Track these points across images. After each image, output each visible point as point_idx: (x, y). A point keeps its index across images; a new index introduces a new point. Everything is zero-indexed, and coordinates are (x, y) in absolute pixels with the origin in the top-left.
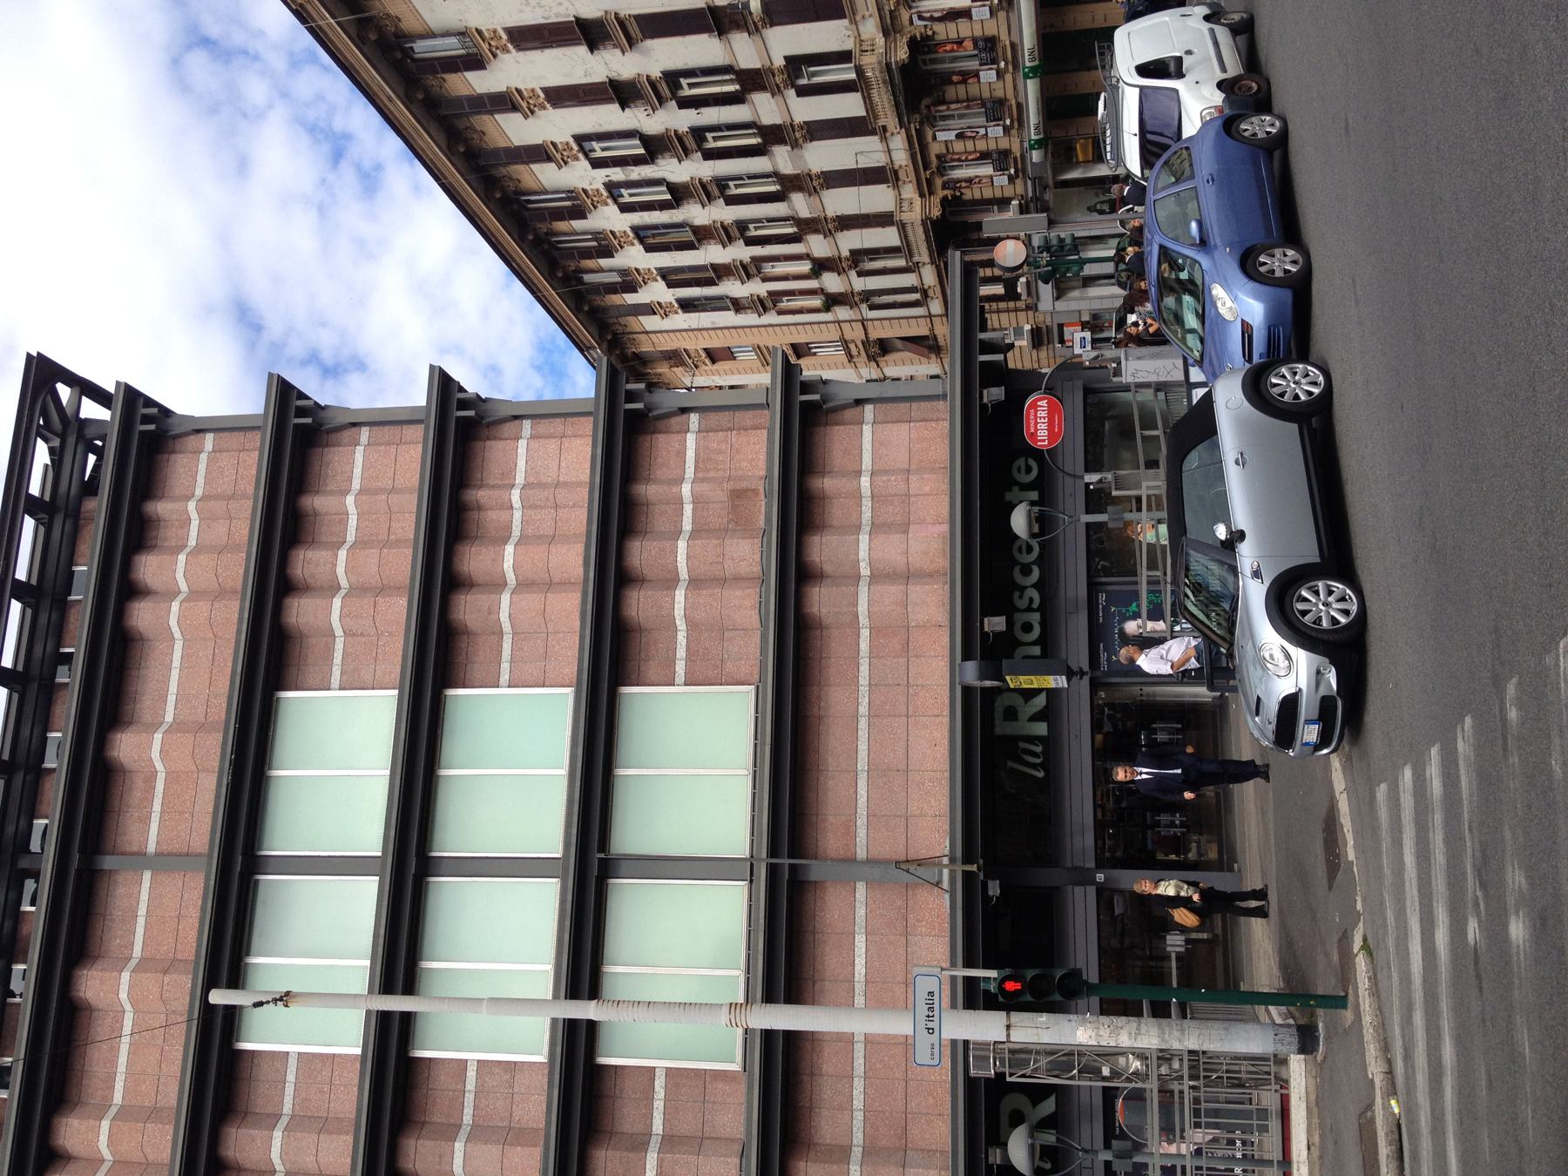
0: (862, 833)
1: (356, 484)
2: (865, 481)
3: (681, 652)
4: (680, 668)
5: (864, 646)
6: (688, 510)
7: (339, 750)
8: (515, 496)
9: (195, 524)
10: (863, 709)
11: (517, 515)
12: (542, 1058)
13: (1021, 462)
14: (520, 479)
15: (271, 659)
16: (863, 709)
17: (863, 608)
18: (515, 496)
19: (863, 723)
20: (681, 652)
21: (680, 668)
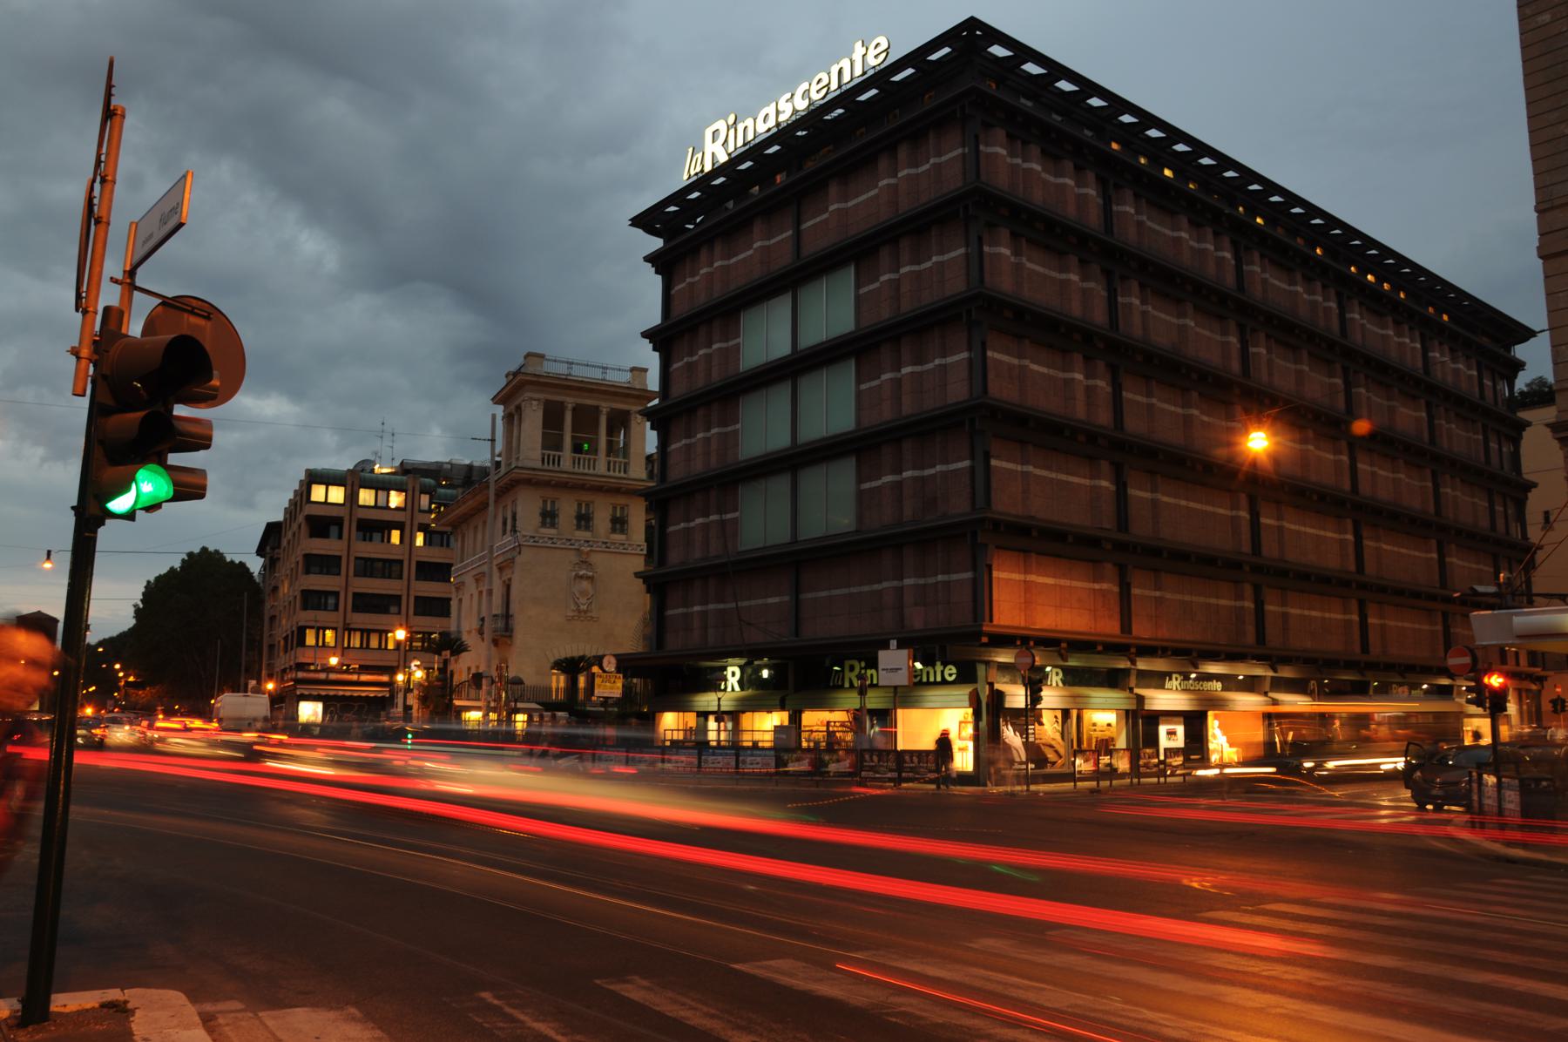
0: (809, 595)
1: (946, 257)
2: (940, 578)
3: (874, 484)
4: (866, 486)
5: (876, 587)
6: (932, 471)
7: (831, 310)
8: (937, 362)
9: (926, 167)
10: (854, 590)
11: (931, 366)
12: (741, 458)
13: (954, 671)
14: (950, 360)
15: (858, 252)
16: (854, 590)
17: (885, 585)
18: (937, 362)
19: (845, 591)
20: (874, 484)
21: (866, 486)
